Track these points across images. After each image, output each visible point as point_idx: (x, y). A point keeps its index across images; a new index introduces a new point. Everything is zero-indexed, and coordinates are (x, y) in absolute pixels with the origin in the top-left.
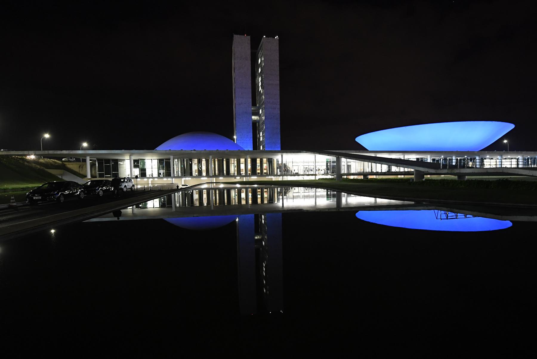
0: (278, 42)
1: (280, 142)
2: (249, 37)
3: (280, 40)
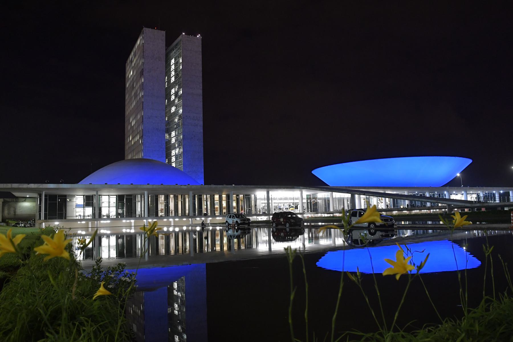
1: (203, 170)
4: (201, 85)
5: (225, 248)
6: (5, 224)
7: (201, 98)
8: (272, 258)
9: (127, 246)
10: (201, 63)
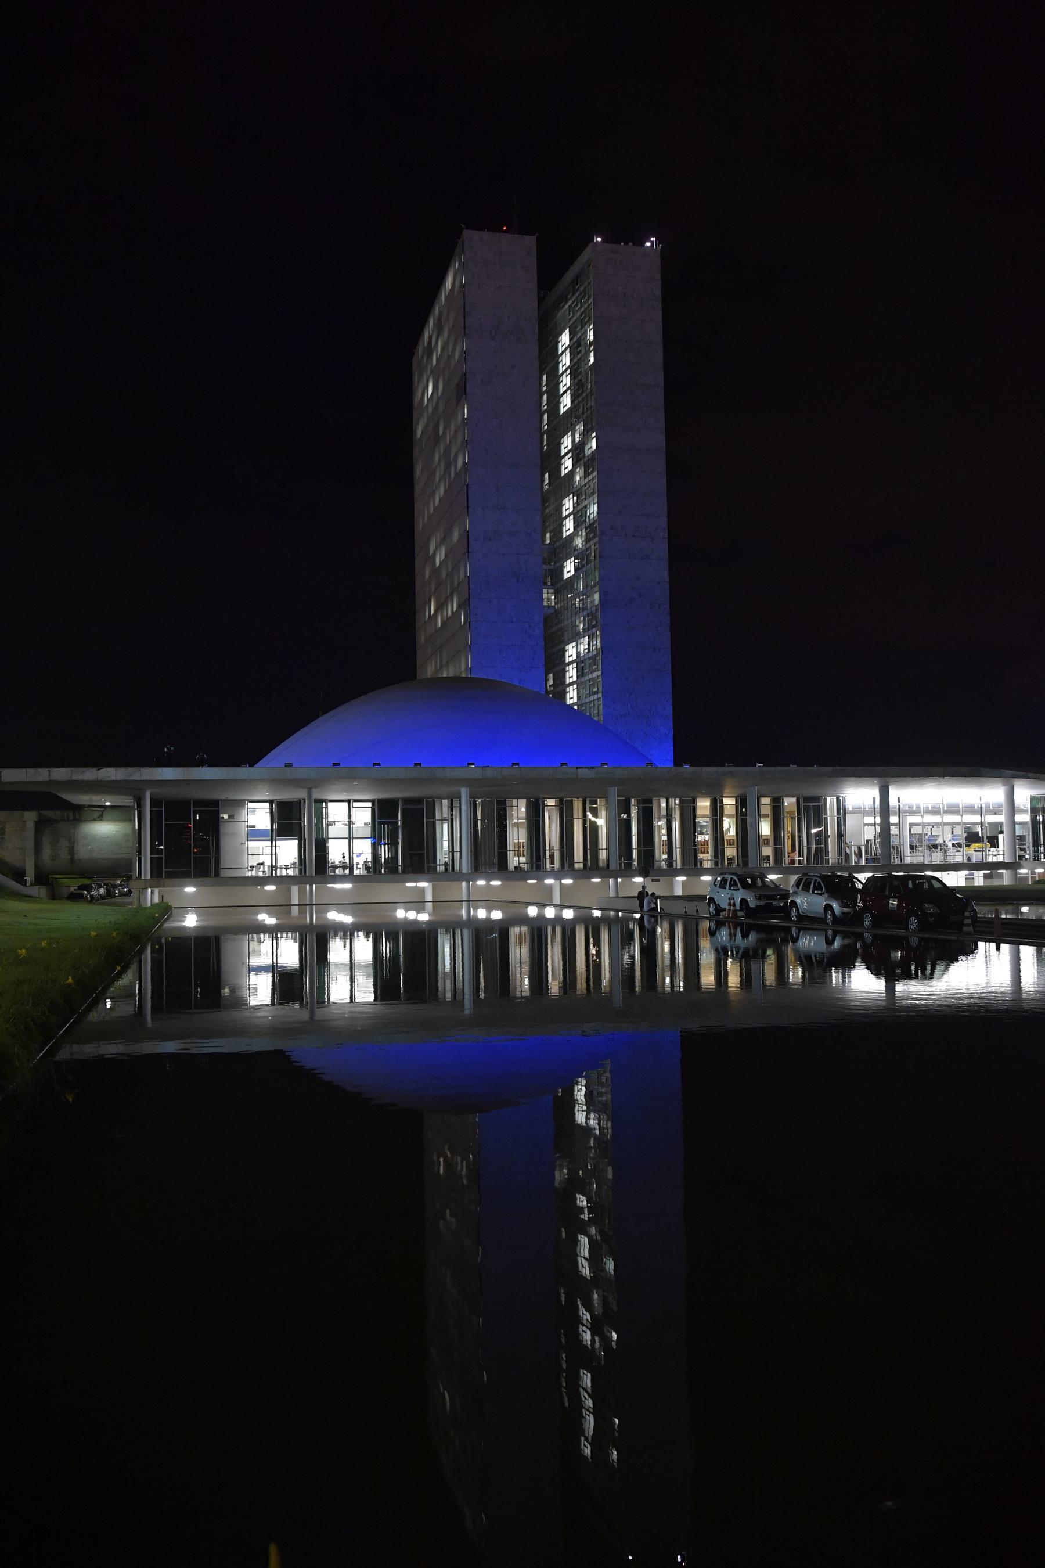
0: (658, 261)
1: (669, 710)
2: (530, 242)
3: (667, 255)
4: (661, 415)
5: (734, 980)
6: (40, 891)
7: (660, 464)
8: (890, 1022)
9: (406, 965)
10: (657, 337)
